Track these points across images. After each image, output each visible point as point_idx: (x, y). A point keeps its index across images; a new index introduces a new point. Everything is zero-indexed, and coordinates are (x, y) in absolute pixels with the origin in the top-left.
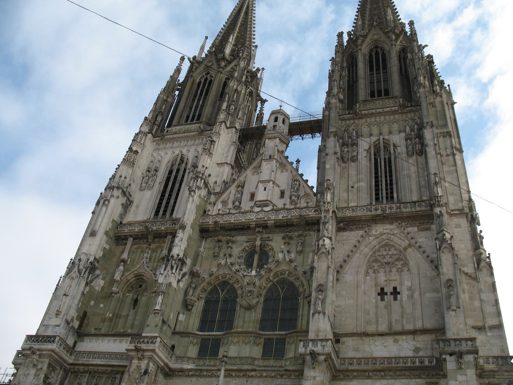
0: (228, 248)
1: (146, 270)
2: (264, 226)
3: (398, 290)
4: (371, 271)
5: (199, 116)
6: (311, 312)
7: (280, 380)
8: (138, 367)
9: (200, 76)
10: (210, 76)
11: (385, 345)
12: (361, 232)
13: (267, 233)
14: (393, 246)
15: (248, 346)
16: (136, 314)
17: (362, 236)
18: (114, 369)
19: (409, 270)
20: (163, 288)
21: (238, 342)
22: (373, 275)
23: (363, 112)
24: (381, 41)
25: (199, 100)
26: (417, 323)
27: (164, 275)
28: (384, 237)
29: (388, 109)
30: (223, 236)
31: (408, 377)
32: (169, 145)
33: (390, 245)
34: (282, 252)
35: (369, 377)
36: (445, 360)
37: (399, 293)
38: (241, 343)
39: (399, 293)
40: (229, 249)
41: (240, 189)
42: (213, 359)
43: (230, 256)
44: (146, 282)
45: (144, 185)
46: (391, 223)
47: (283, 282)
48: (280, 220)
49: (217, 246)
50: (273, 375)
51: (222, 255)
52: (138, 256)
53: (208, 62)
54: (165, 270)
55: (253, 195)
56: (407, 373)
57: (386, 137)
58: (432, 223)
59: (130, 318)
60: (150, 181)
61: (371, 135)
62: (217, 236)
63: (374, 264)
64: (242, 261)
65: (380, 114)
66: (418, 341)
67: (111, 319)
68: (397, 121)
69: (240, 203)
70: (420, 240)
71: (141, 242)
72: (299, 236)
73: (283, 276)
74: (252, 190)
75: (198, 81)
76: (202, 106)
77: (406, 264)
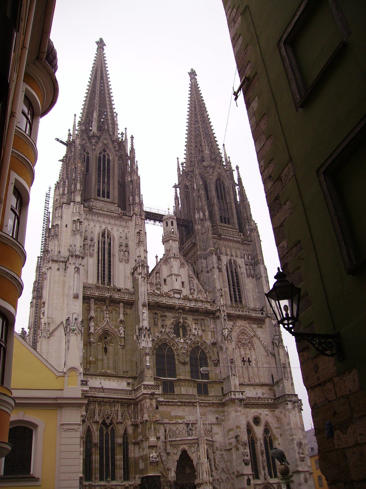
0: (163, 320)
1: (111, 327)
2: (183, 309)
3: (250, 360)
4: (237, 347)
5: (108, 193)
6: (230, 375)
7: (209, 408)
8: (151, 404)
9: (99, 152)
10: (107, 154)
11: (250, 390)
12: (232, 323)
13: (183, 313)
14: (246, 334)
15: (191, 388)
16: (108, 359)
17: (233, 326)
18: (115, 400)
19: (254, 349)
20: (147, 351)
21: (185, 385)
22: (239, 350)
23: (223, 236)
24: (222, 175)
25: (104, 175)
26: (261, 380)
27: (145, 341)
28: (242, 327)
29: (236, 239)
30: (158, 310)
31: (263, 408)
32: (95, 218)
33: (244, 333)
34: (195, 329)
35: (248, 407)
36: (287, 404)
37: (250, 362)
38: (187, 386)
39: (250, 362)
40: (164, 321)
41: (158, 275)
42: (172, 394)
43: (166, 326)
44: (110, 335)
45: (86, 251)
46: (245, 320)
47: (198, 348)
48: (192, 307)
49: (157, 317)
50: (207, 405)
51: (160, 324)
52: (99, 314)
53: (104, 139)
54: (144, 337)
55: (165, 280)
56: (264, 406)
57: (235, 258)
58: (263, 324)
59: (105, 361)
60: (91, 250)
61: (227, 255)
62: (154, 309)
63: (238, 343)
64: (172, 331)
65: (230, 240)
66: (263, 389)
67: (95, 363)
68: (239, 249)
69: (160, 286)
70: (259, 333)
71: (99, 304)
72: (202, 319)
73: (198, 345)
74: (166, 278)
75: (98, 155)
76: (108, 184)
77: (253, 346)
